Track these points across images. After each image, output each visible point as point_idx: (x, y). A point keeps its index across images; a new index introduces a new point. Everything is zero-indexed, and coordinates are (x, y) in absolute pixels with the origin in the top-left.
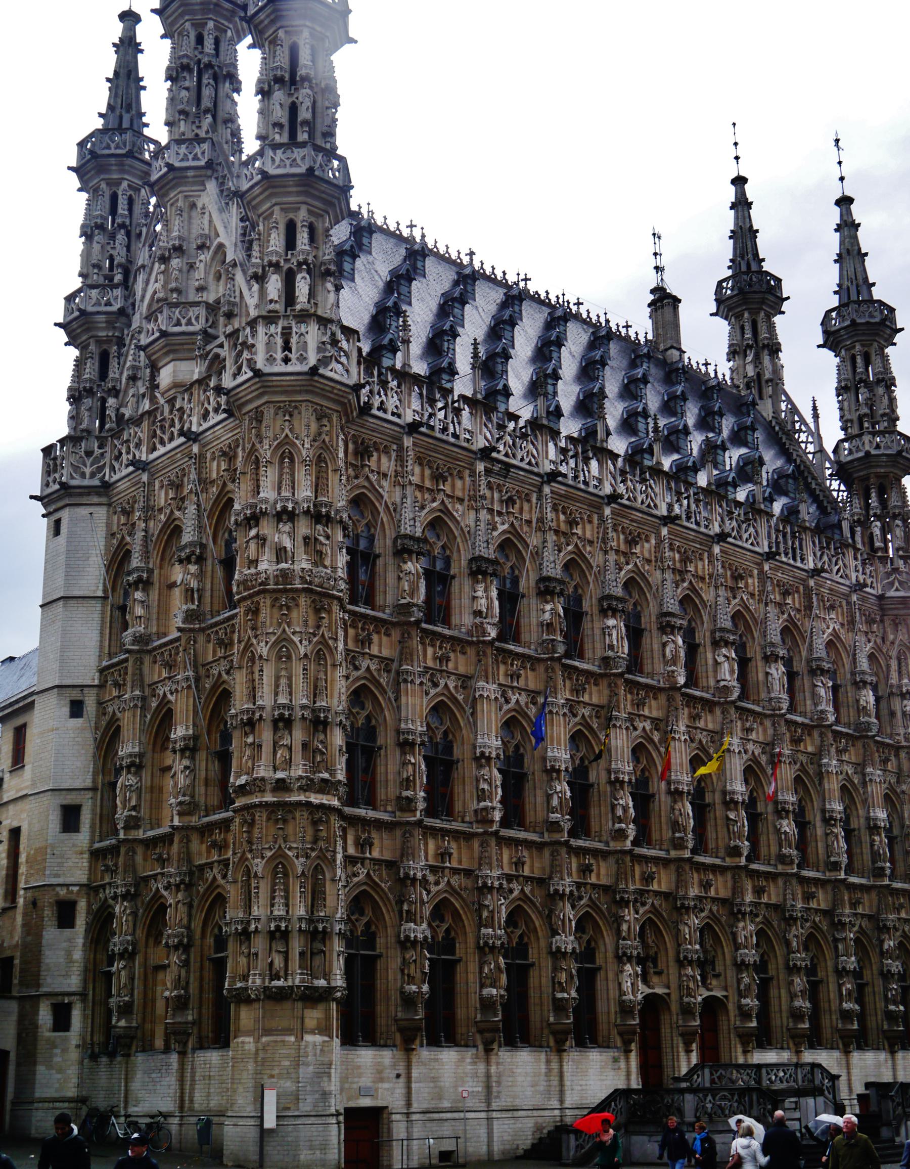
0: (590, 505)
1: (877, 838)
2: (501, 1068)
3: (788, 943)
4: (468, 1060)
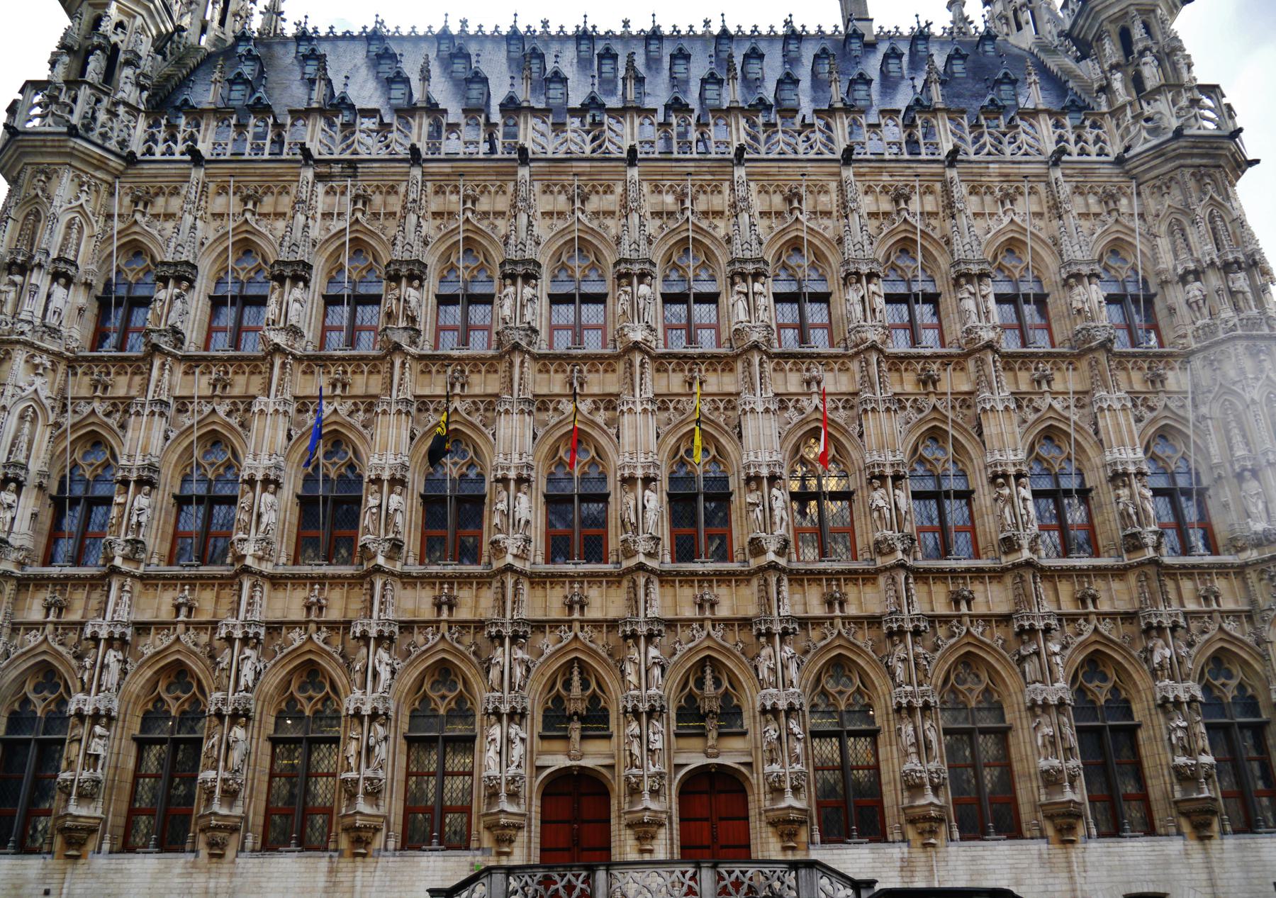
0: (498, 174)
1: (1124, 492)
2: (238, 881)
3: (893, 675)
4: (178, 871)
